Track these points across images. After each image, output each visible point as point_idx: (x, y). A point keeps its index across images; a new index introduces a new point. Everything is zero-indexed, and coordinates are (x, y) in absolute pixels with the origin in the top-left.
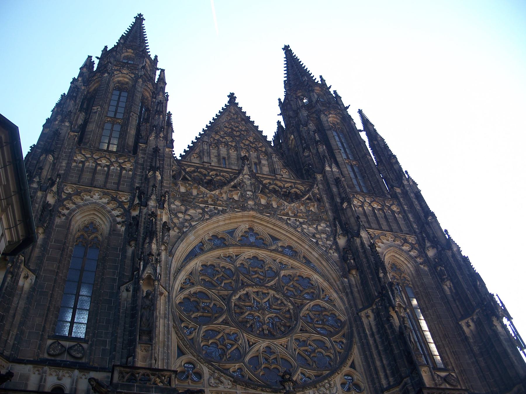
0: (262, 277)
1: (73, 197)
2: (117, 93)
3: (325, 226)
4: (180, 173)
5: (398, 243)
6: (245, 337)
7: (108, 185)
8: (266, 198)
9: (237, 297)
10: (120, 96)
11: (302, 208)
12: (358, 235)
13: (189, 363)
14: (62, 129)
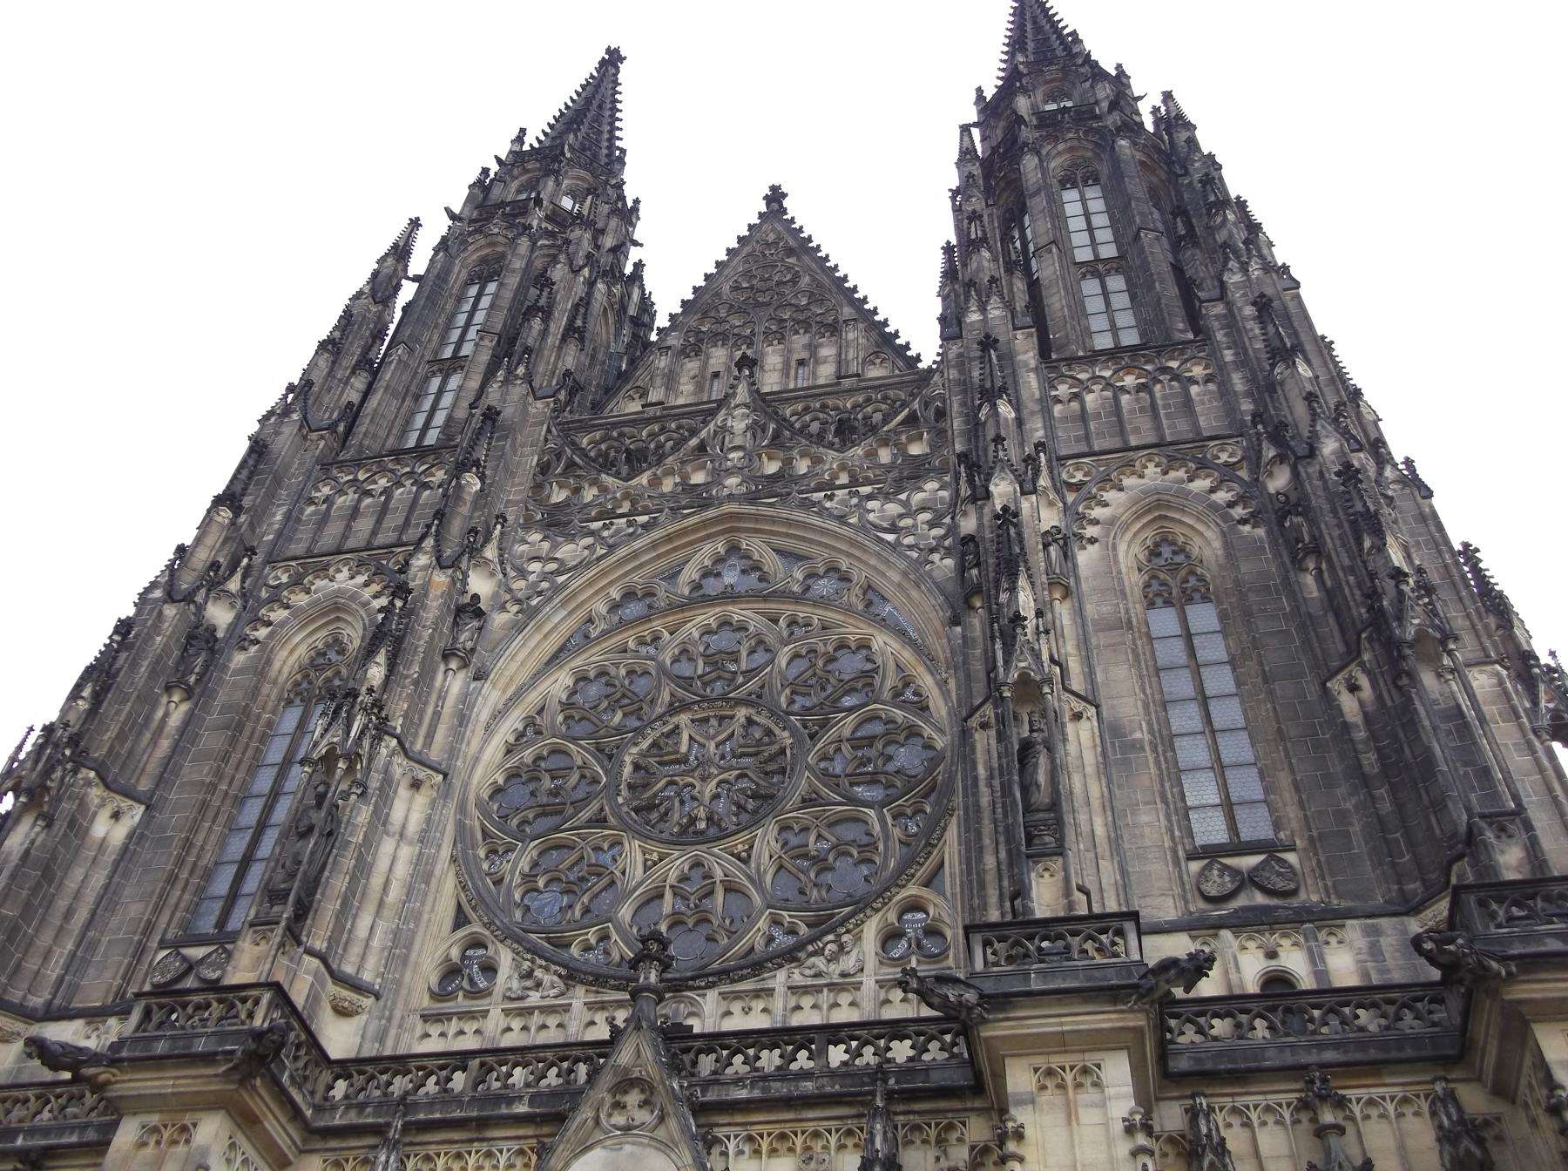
0: (727, 675)
1: (285, 593)
3: (936, 485)
4: (558, 457)
9: (645, 745)
13: (477, 943)
14: (277, 433)
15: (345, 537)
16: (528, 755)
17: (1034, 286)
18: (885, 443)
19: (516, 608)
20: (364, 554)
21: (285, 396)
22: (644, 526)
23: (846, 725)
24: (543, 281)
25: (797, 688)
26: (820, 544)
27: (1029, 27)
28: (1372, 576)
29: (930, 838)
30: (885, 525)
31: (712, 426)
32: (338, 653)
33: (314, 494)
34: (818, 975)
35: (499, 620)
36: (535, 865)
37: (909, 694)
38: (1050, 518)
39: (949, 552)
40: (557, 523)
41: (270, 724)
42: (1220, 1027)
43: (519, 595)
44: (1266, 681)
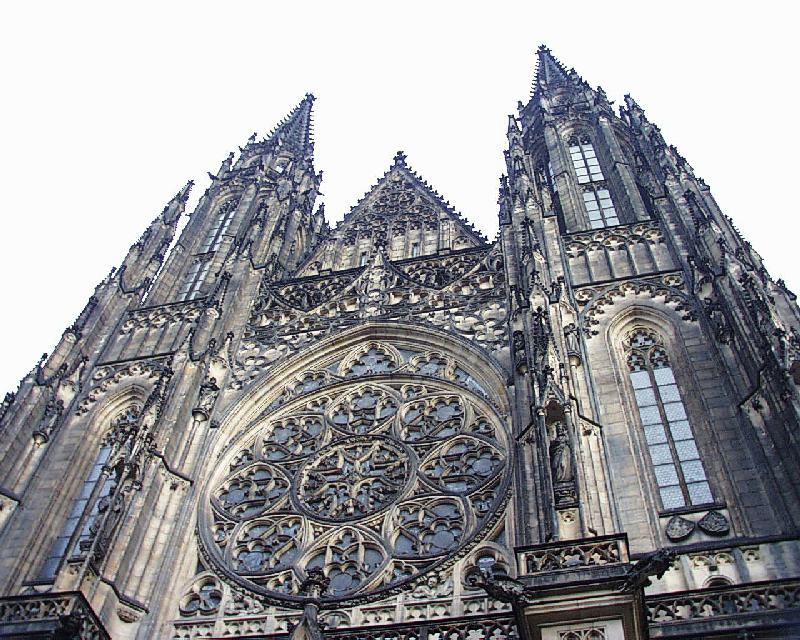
3: (498, 306)
5: (647, 293)
8: (404, 293)
9: (316, 464)
15: (139, 351)
16: (244, 473)
17: (555, 196)
18: (466, 283)
19: (238, 386)
20: (151, 359)
21: (111, 274)
22: (317, 337)
23: (445, 449)
24: (263, 206)
25: (412, 428)
27: (547, 70)
28: (763, 335)
29: (497, 513)
30: (466, 329)
31: (360, 279)
33: (123, 328)
35: (227, 393)
36: (246, 535)
37: (482, 428)
38: (567, 320)
39: (506, 343)
40: (263, 337)
42: (683, 611)
43: (240, 379)
44: (704, 408)
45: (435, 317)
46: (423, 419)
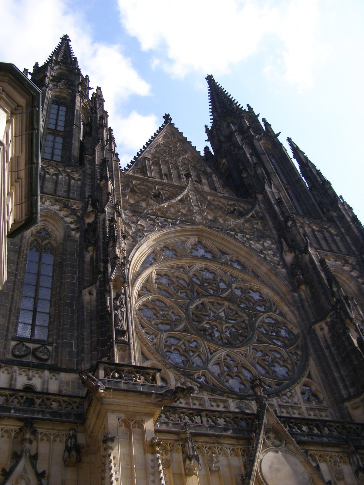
2: (56, 107)
5: (340, 263)
6: (204, 345)
7: (59, 193)
8: (213, 214)
9: (194, 306)
10: (58, 110)
11: (246, 225)
12: (306, 251)
18: (246, 221)
26: (233, 250)
32: (47, 234)
34: (287, 402)
36: (166, 342)
37: (277, 312)
41: (26, 255)
45: (238, 236)
46: (245, 296)
